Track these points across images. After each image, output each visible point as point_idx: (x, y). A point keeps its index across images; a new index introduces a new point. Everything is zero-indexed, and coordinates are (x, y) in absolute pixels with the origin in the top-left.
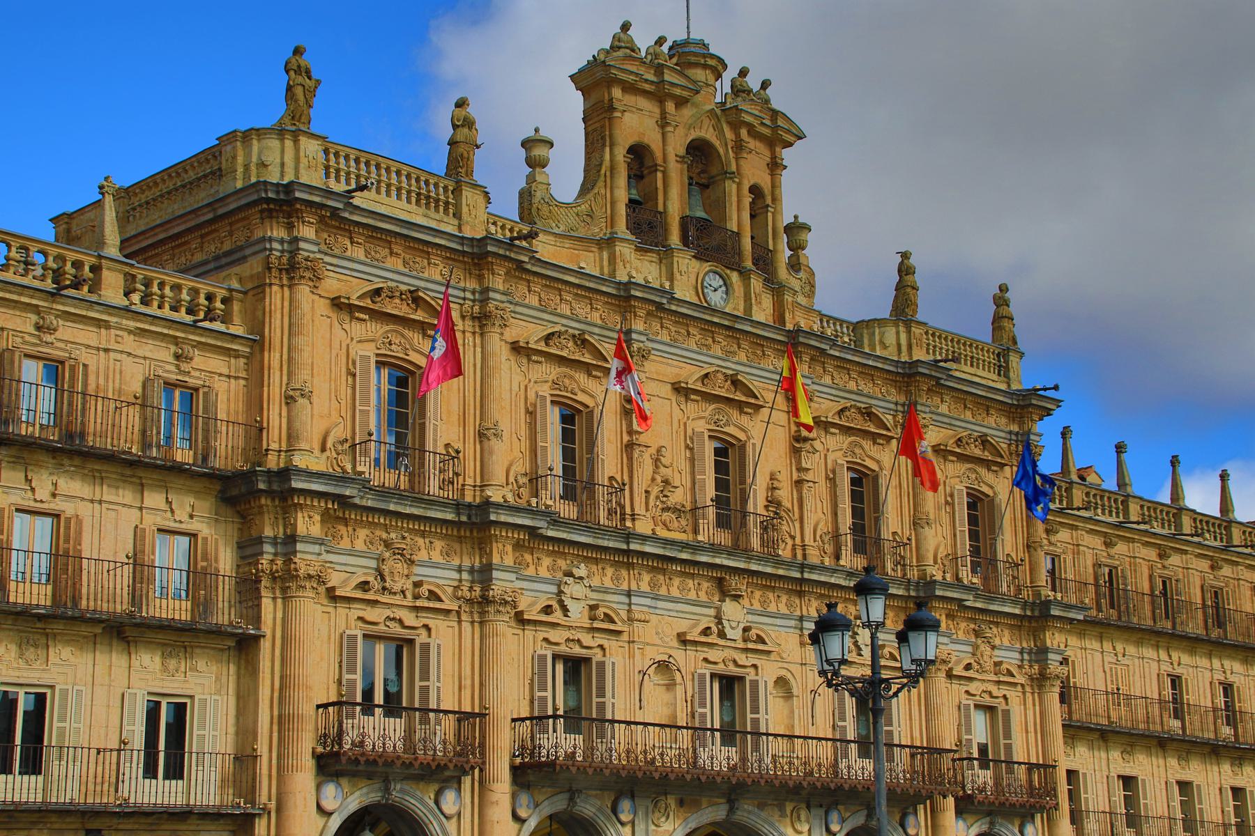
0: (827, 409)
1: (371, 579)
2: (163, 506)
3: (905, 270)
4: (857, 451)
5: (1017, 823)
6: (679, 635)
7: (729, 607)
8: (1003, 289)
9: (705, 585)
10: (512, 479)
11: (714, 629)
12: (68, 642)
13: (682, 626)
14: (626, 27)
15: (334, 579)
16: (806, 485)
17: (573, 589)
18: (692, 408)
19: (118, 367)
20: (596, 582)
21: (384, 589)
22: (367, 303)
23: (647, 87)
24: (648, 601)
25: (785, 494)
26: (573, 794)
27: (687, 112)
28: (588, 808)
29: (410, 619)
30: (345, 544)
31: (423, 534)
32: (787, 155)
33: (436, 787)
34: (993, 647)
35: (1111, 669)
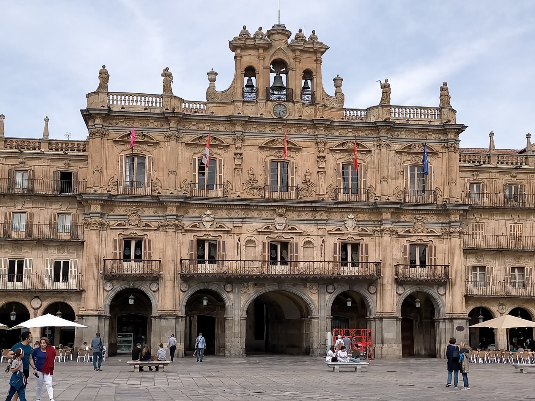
4: (351, 158)
5: (436, 289)
7: (278, 219)
8: (445, 84)
14: (245, 27)
15: (112, 222)
16: (320, 173)
17: (207, 219)
18: (266, 153)
19: (44, 170)
20: (219, 215)
21: (130, 224)
23: (251, 46)
24: (241, 220)
25: (313, 178)
28: (214, 288)
30: (116, 212)
32: (323, 57)
33: (150, 282)
34: (424, 223)
35: (511, 226)
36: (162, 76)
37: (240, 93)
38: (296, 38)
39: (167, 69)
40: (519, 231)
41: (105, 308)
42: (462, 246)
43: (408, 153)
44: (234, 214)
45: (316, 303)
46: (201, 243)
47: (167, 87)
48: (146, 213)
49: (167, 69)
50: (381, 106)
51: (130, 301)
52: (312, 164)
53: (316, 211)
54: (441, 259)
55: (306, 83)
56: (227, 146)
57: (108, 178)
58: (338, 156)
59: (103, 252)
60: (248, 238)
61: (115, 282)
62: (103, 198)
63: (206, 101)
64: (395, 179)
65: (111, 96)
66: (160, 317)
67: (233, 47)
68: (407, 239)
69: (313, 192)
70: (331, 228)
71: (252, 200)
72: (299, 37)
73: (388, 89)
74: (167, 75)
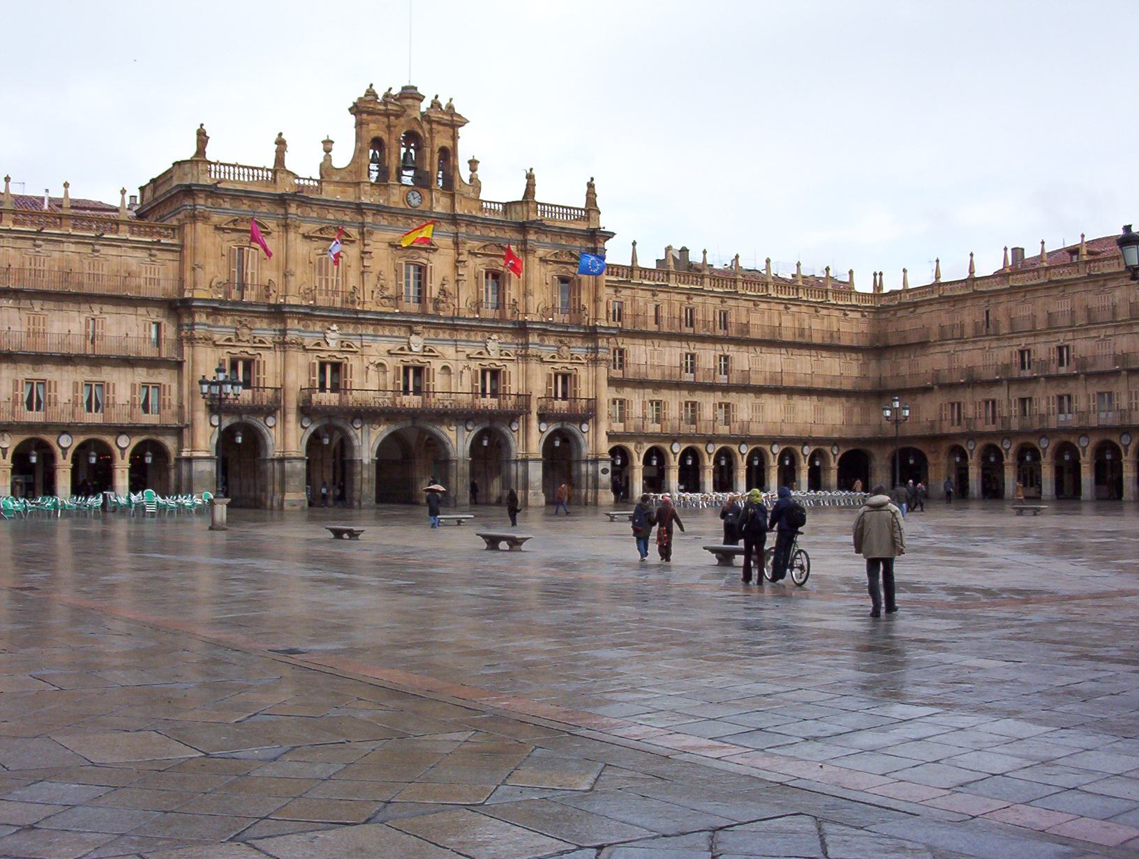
0: (475, 245)
2: (145, 313)
3: (530, 177)
6: (389, 351)
7: (413, 338)
8: (592, 179)
9: (403, 329)
10: (301, 291)
11: (406, 347)
12: (108, 365)
13: (390, 346)
14: (371, 85)
15: (216, 337)
17: (333, 335)
20: (344, 332)
22: (232, 226)
23: (379, 112)
24: (371, 338)
25: (450, 287)
26: (330, 417)
27: (402, 120)
28: (340, 423)
29: (251, 351)
30: (221, 323)
31: (257, 317)
32: (460, 130)
36: (276, 143)
38: (432, 106)
39: (280, 134)
44: (361, 330)
45: (454, 442)
47: (280, 160)
48: (258, 326)
49: (280, 134)
53: (456, 330)
54: (584, 391)
56: (353, 242)
58: (478, 261)
62: (214, 305)
63: (318, 177)
65: (213, 166)
66: (282, 460)
67: (356, 109)
69: (451, 306)
72: (435, 104)
73: (531, 180)
74: (281, 143)
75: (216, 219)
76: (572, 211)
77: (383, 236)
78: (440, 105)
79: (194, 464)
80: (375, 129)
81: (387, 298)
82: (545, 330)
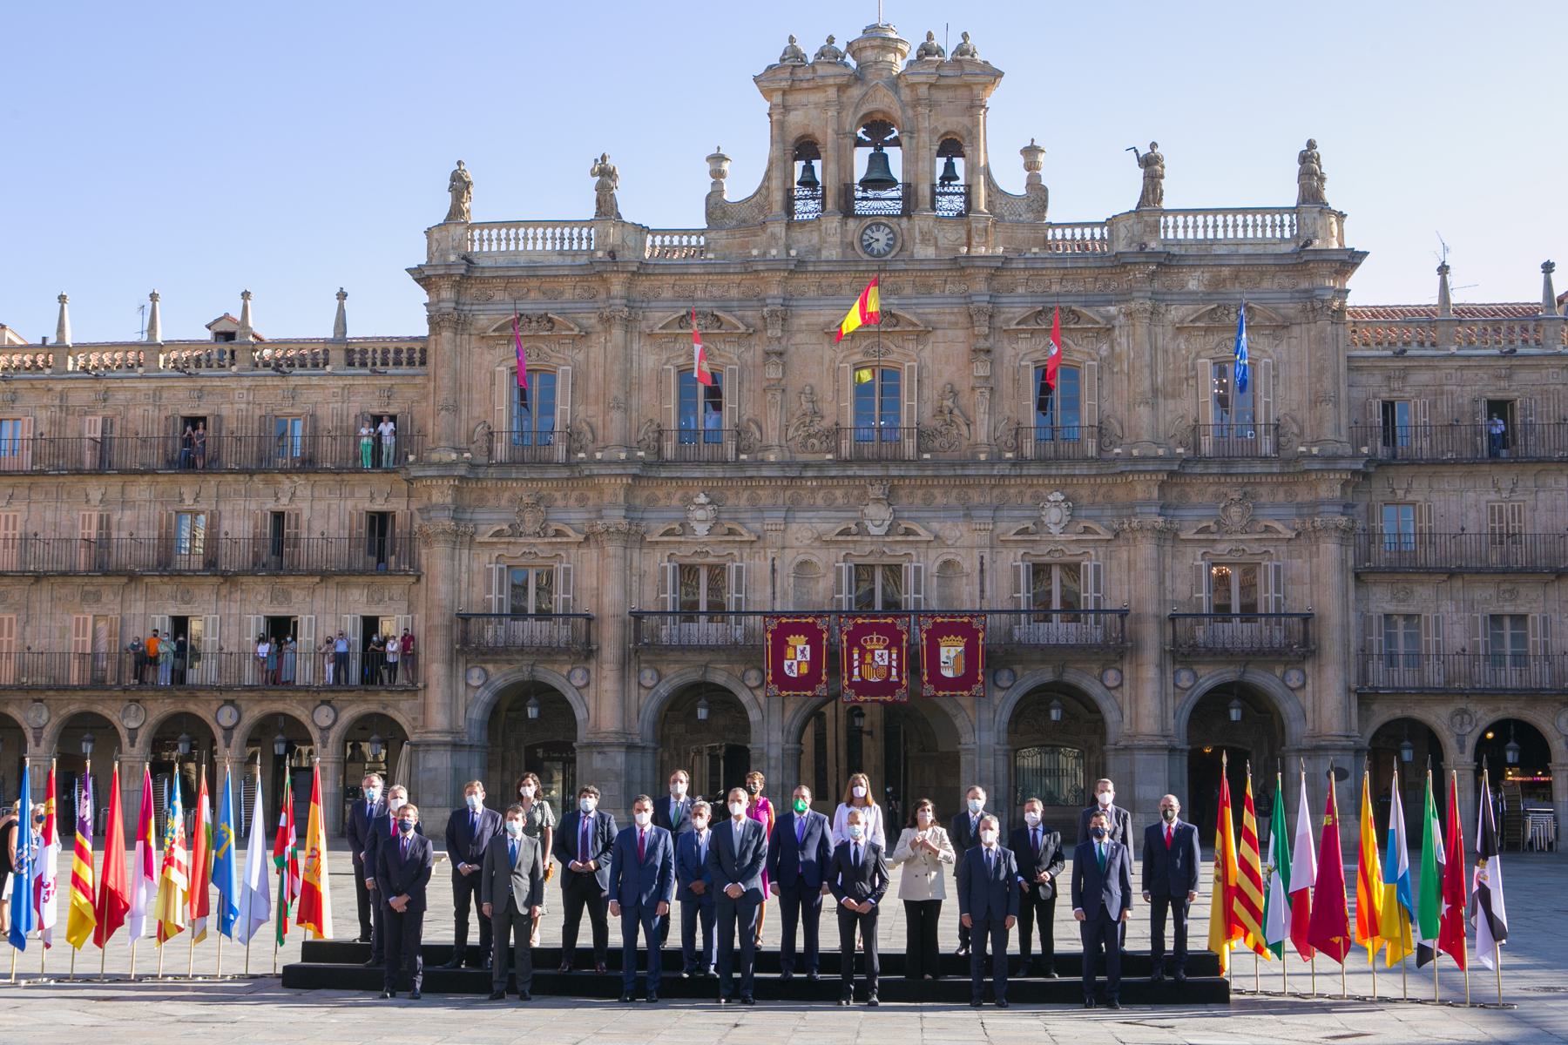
1: (505, 527)
7: (872, 510)
8: (1311, 144)
11: (853, 527)
14: (791, 39)
17: (700, 514)
35: (1493, 508)
37: (779, 204)
38: (919, 57)
39: (604, 158)
40: (1513, 519)
41: (470, 725)
42: (1351, 563)
43: (1207, 330)
44: (765, 496)
46: (687, 572)
49: (604, 158)
50: (1138, 212)
51: (529, 710)
52: (959, 370)
55: (949, 167)
57: (472, 425)
59: (464, 599)
60: (801, 558)
61: (490, 667)
63: (705, 226)
64: (1173, 397)
65: (477, 233)
66: (590, 746)
68: (1204, 550)
70: (1008, 527)
71: (806, 465)
74: (605, 174)
75: (482, 320)
76: (1278, 217)
77: (813, 320)
78: (939, 51)
79: (421, 755)
80: (805, 118)
81: (815, 436)
82: (1171, 474)
